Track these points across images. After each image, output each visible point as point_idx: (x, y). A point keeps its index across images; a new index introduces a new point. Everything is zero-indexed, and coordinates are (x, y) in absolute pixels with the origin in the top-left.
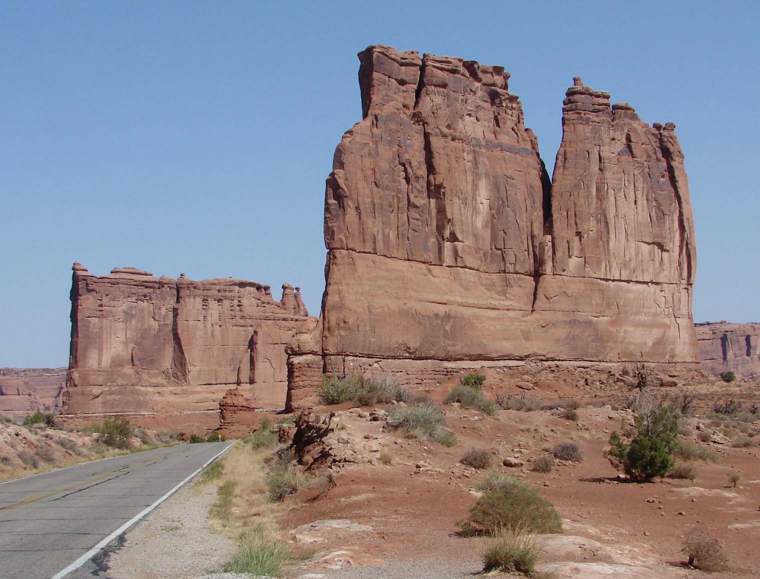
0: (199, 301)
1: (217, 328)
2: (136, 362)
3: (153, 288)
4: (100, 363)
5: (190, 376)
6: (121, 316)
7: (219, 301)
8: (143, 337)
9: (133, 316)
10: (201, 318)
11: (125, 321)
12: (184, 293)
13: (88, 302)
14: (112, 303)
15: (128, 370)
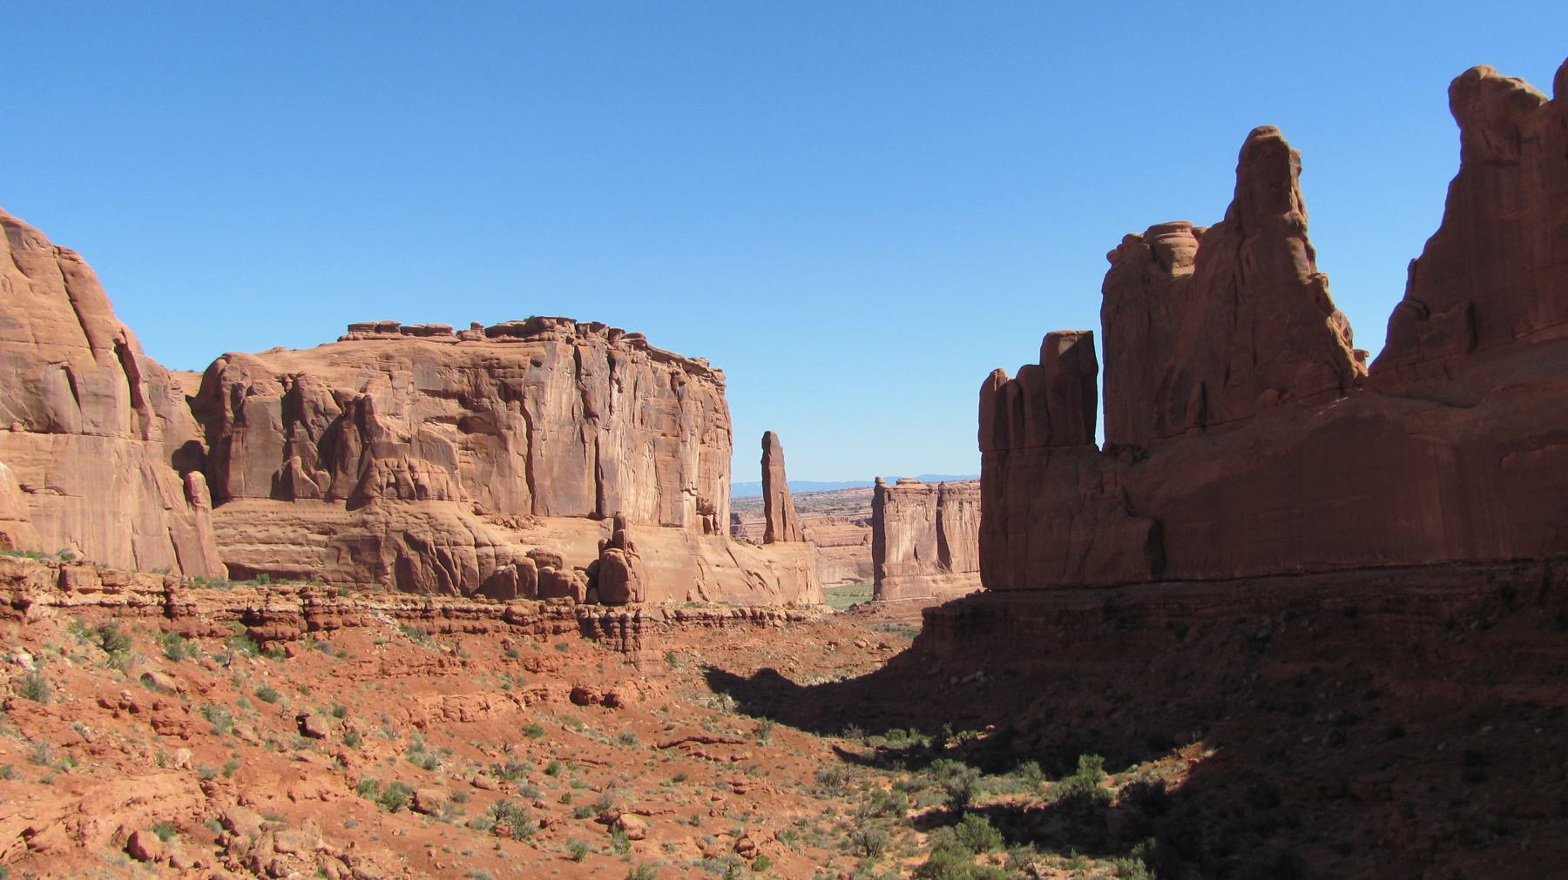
0: (957, 503)
1: (969, 525)
2: (919, 557)
3: (926, 494)
4: (897, 558)
5: (953, 566)
6: (908, 520)
7: (971, 503)
8: (921, 535)
9: (915, 518)
10: (958, 517)
11: (912, 523)
12: (946, 496)
13: (890, 508)
14: (904, 509)
15: (914, 562)
